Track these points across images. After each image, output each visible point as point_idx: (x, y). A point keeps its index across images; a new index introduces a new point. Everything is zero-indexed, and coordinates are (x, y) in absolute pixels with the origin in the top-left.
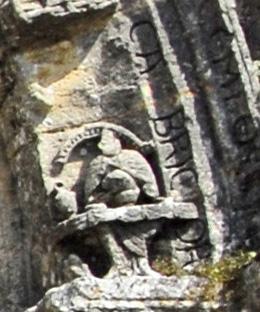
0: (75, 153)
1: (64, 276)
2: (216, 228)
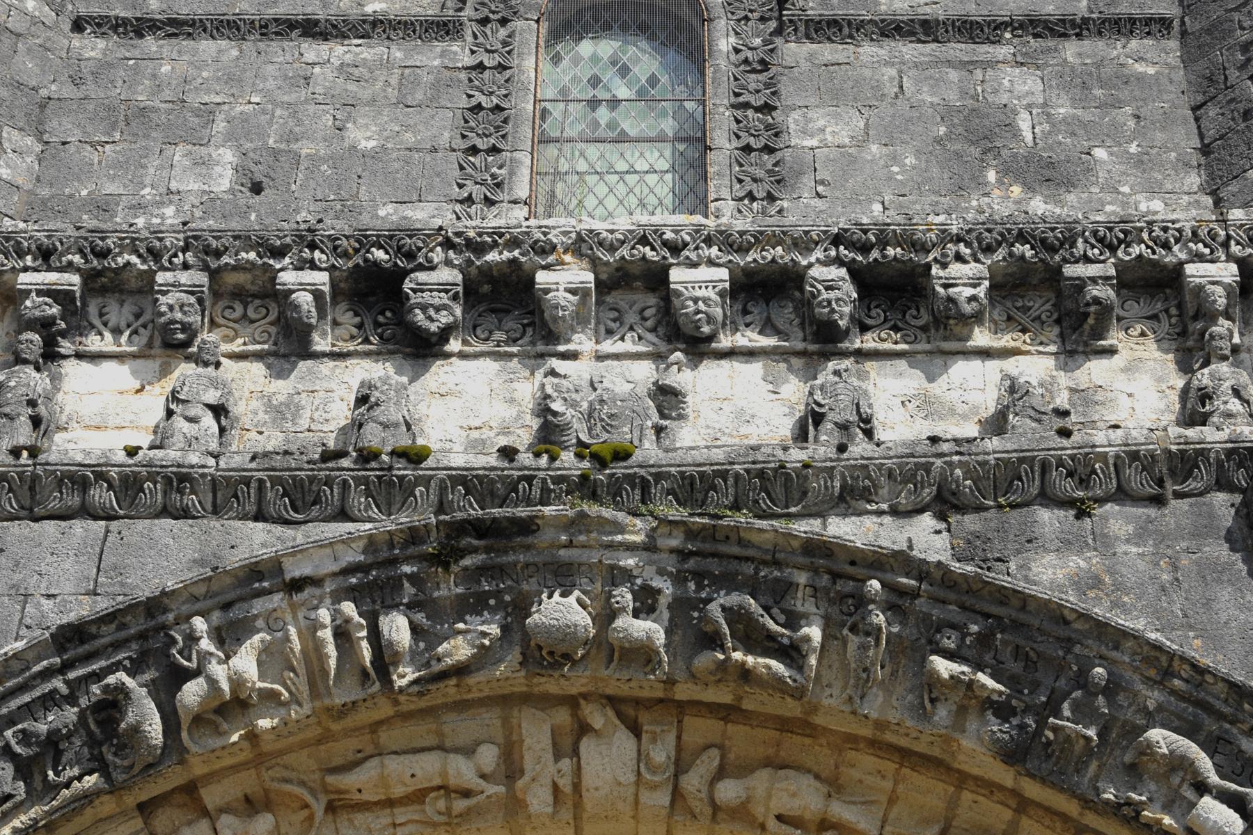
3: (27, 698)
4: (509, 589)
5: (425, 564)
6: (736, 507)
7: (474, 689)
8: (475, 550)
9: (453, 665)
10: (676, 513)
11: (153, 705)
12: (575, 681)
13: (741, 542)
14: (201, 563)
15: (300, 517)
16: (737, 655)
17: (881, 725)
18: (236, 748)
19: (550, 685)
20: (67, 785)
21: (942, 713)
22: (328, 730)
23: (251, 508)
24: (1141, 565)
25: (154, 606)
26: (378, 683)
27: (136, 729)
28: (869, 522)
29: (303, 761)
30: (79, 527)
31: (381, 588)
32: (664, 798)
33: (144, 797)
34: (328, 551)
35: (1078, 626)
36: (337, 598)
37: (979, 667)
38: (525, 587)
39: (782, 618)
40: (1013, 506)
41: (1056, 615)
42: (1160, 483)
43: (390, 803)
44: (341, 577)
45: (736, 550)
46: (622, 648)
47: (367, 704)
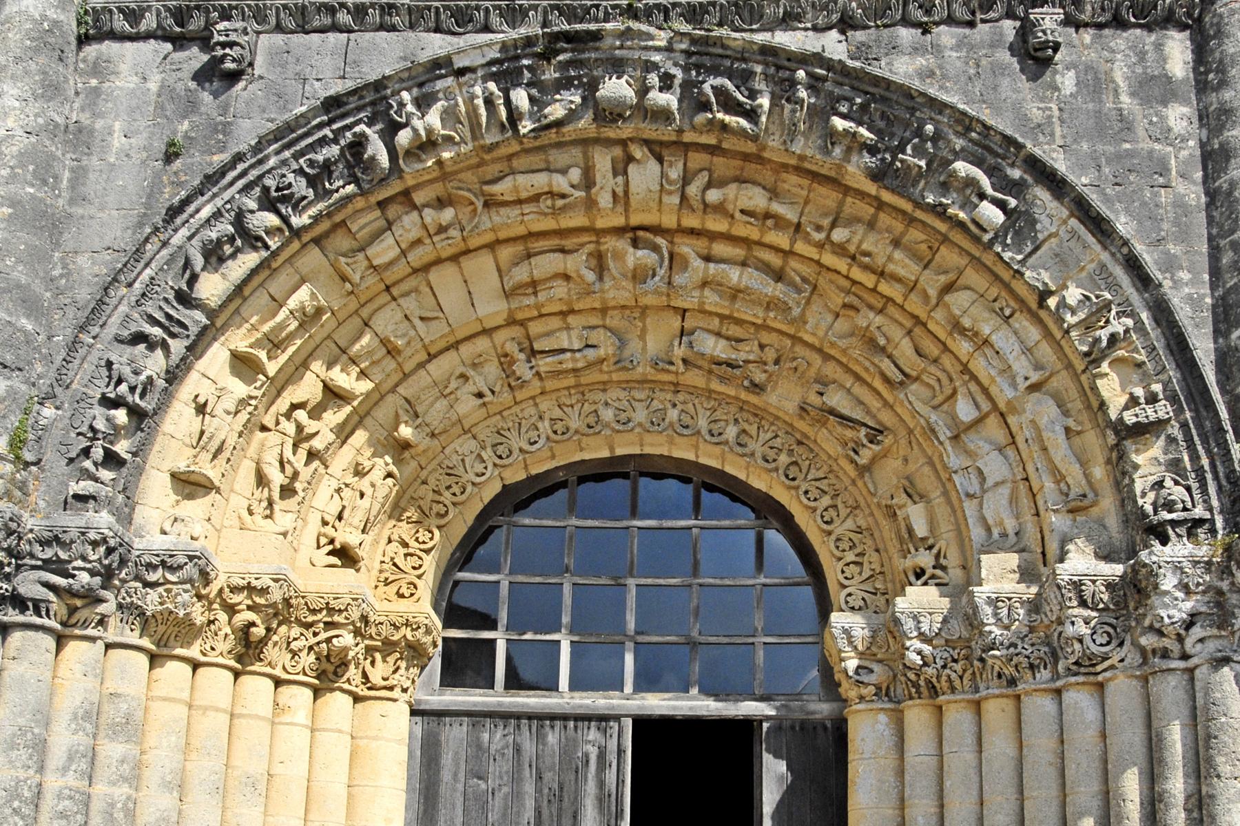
0: (1153, 488)
1: (1147, 546)
2: (1219, 523)
3: (310, 140)
4: (586, 75)
6: (720, 25)
8: (565, 51)
10: (685, 28)
12: (625, 130)
13: (723, 46)
14: (405, 59)
15: (461, 30)
16: (720, 116)
17: (802, 158)
19: (610, 133)
20: (337, 191)
21: (837, 151)
22: (482, 159)
23: (432, 25)
24: (958, 64)
25: (379, 85)
27: (373, 159)
28: (800, 35)
29: (469, 176)
30: (332, 37)
32: (676, 200)
33: (381, 197)
35: (919, 100)
36: (485, 79)
37: (860, 123)
38: (595, 73)
39: (746, 93)
40: (885, 26)
41: (907, 93)
42: (973, 13)
43: (520, 202)
45: (720, 51)
46: (653, 111)
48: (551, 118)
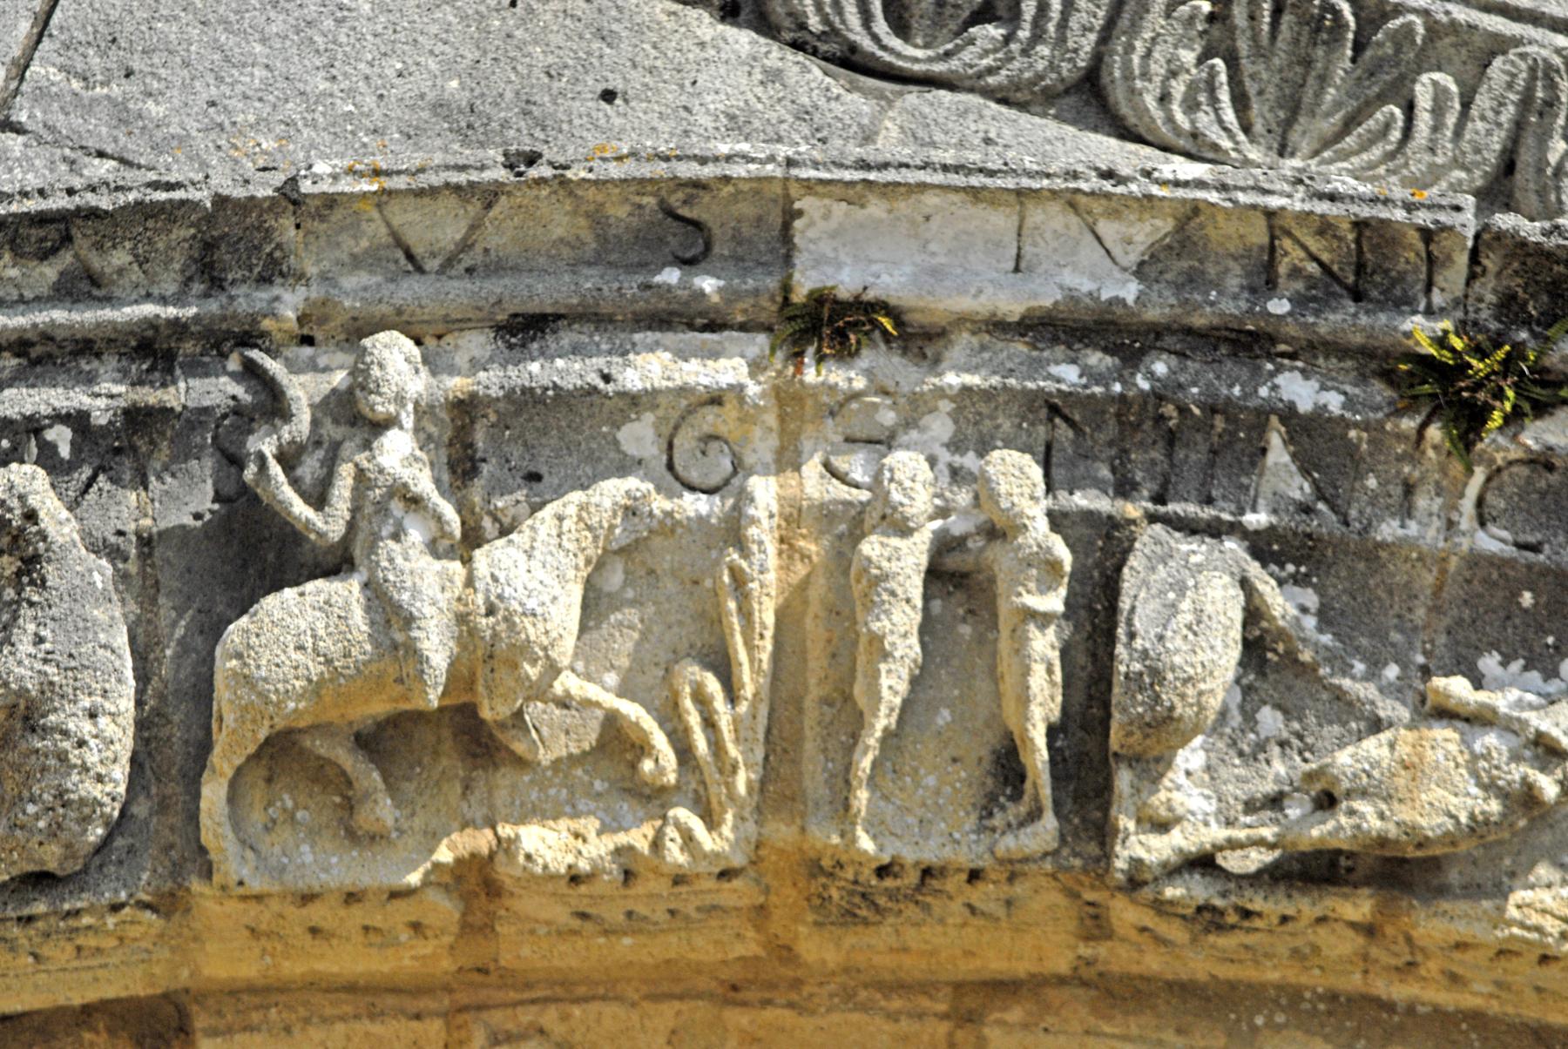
5: (1380, 392)
7: (1432, 967)
9: (1383, 841)
11: (122, 640)
15: (911, 54)
18: (404, 911)
22: (785, 953)
26: (1049, 822)
31: (1171, 439)
34: (1001, 221)
44: (1020, 347)
47: (980, 895)
48: (1369, 817)
